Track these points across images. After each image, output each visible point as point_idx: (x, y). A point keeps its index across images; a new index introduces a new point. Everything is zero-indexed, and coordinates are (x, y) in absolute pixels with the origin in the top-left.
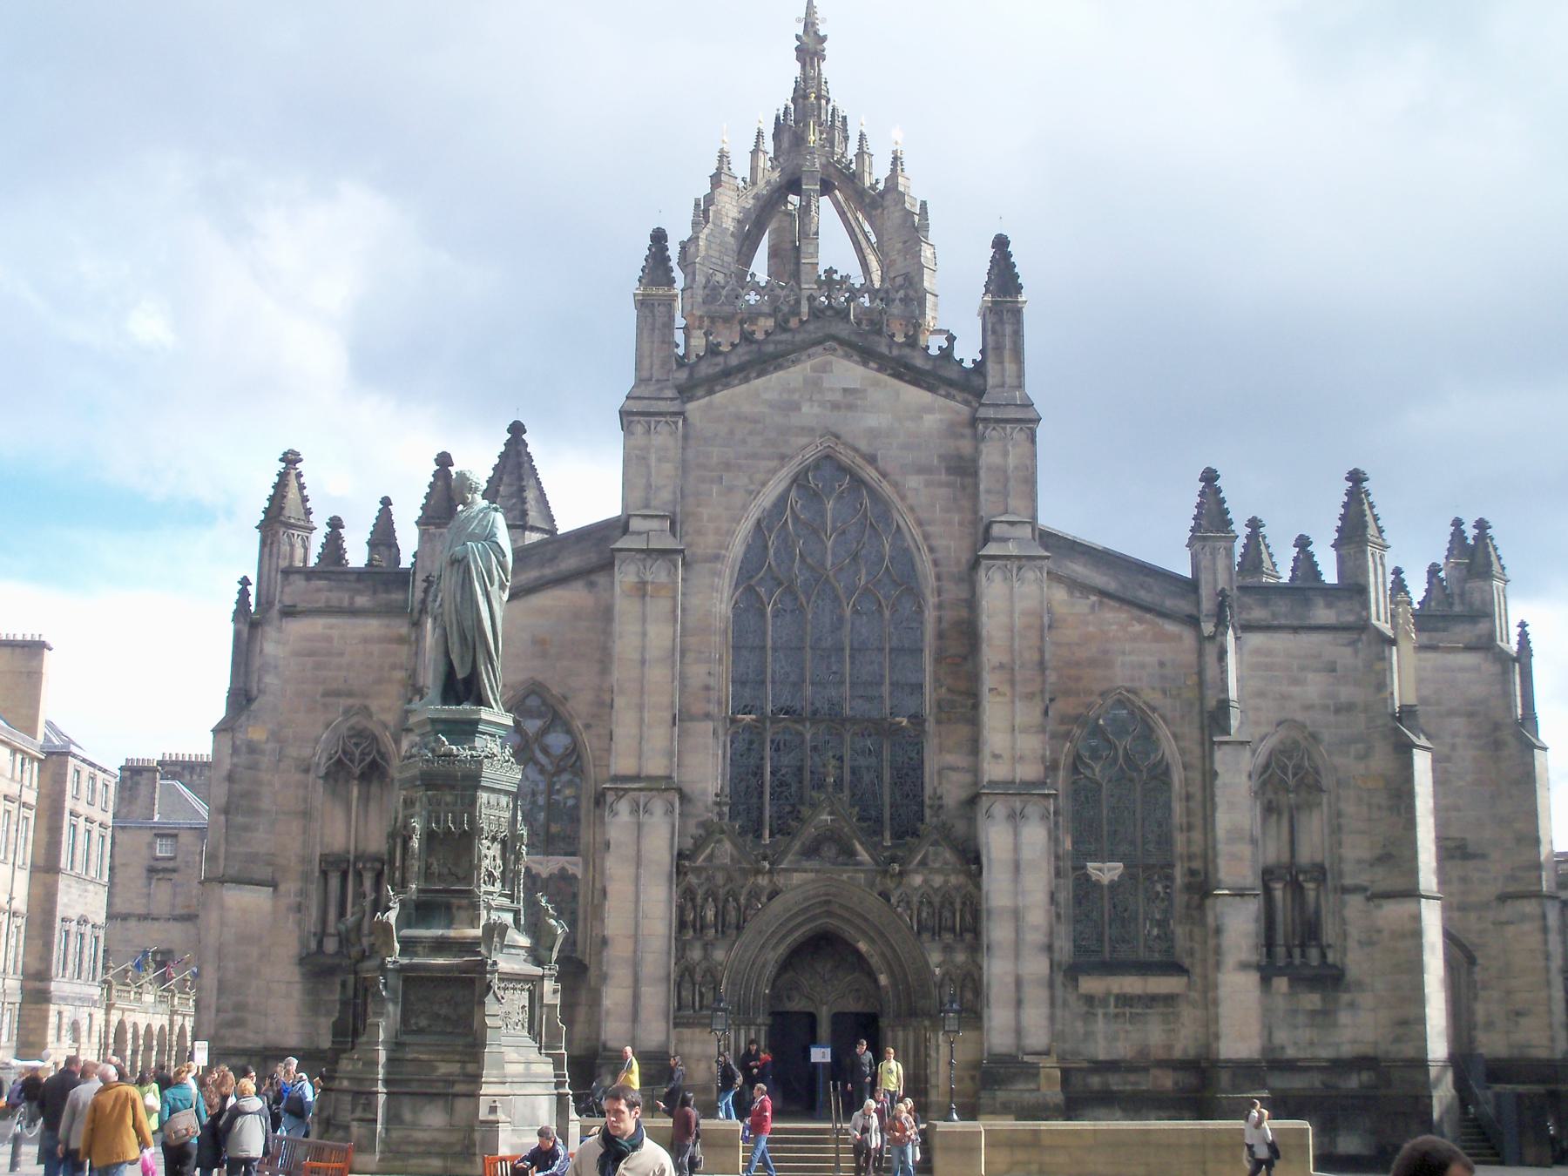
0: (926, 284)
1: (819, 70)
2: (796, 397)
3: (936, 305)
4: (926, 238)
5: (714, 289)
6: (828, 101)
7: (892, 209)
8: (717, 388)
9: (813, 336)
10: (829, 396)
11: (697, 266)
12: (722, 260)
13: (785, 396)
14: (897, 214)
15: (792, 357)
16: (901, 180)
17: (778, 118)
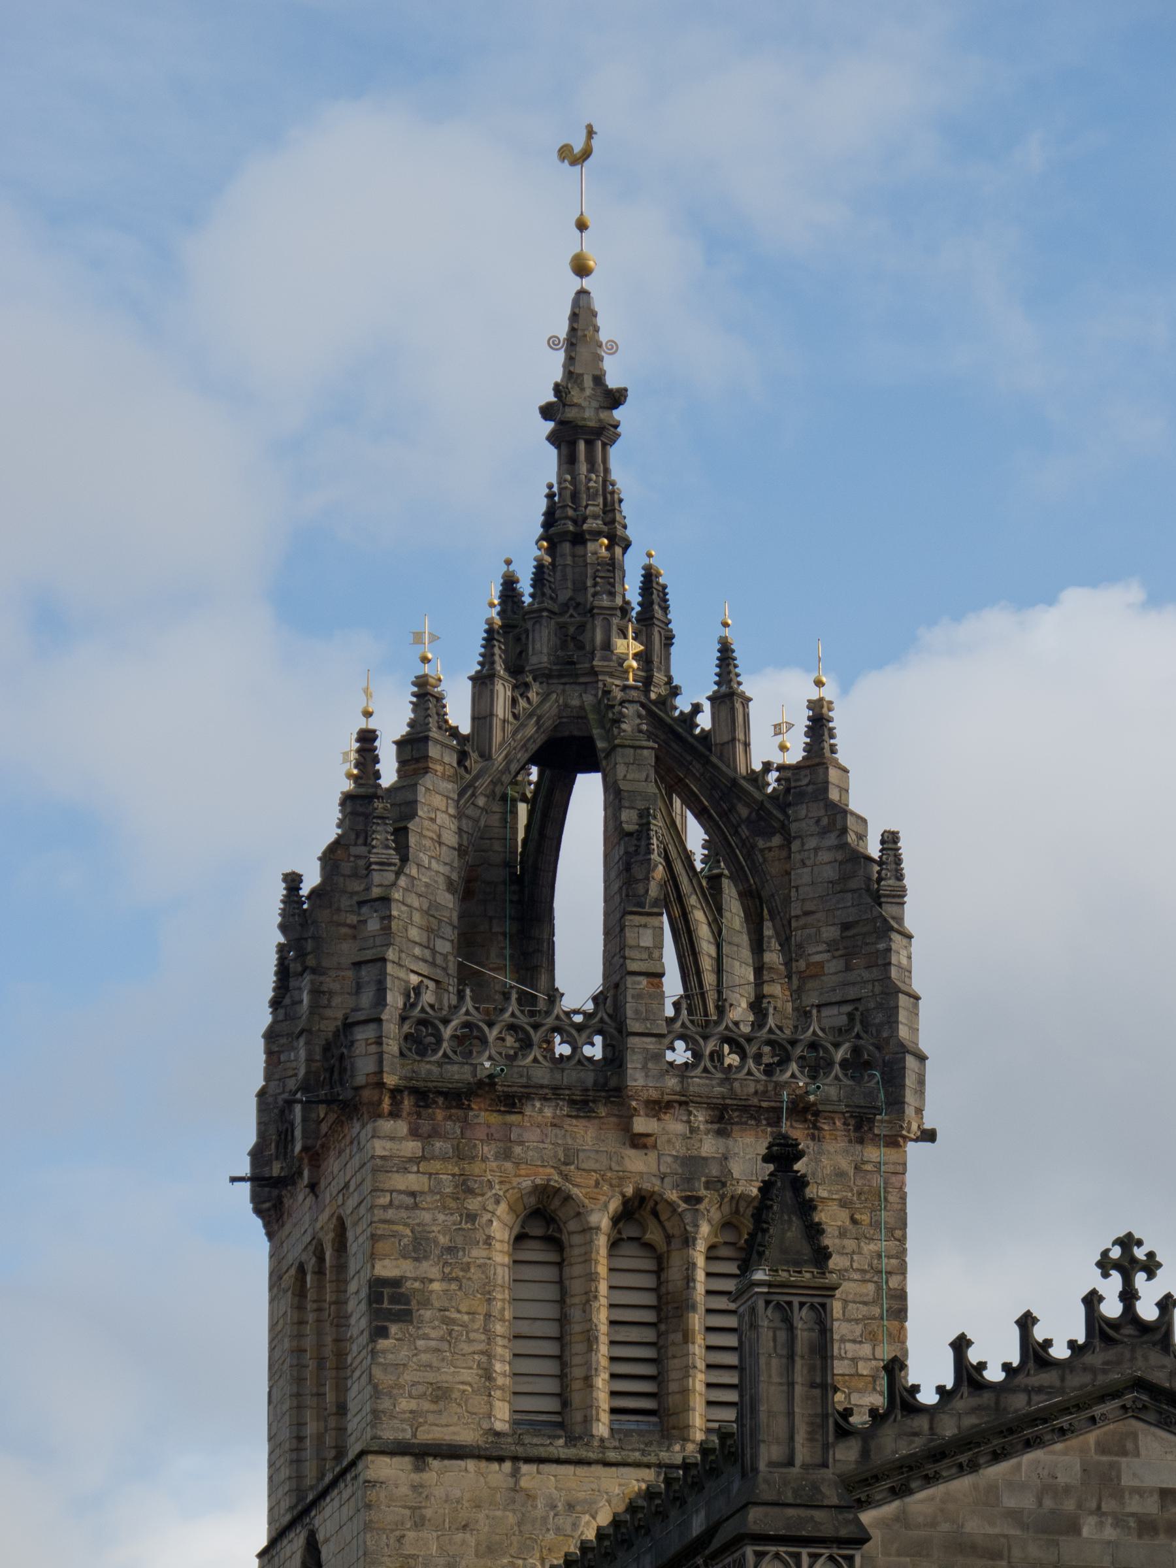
0: (903, 1032)
1: (607, 471)
2: (1069, 1505)
3: (921, 1082)
4: (900, 920)
5: (423, 1022)
6: (627, 545)
7: (812, 843)
8: (914, 1485)
9: (1101, 1379)
10: (1134, 1505)
11: (390, 968)
12: (434, 952)
13: (1048, 1503)
14: (825, 856)
15: (1063, 1421)
16: (833, 774)
17: (509, 585)
